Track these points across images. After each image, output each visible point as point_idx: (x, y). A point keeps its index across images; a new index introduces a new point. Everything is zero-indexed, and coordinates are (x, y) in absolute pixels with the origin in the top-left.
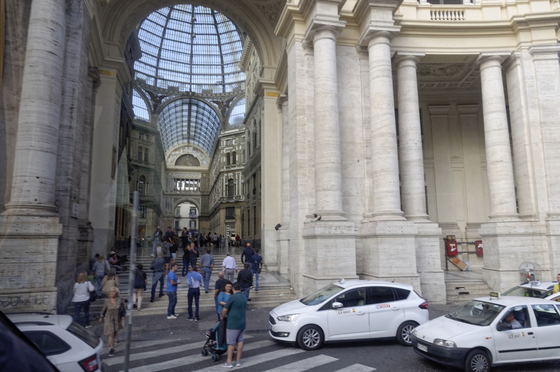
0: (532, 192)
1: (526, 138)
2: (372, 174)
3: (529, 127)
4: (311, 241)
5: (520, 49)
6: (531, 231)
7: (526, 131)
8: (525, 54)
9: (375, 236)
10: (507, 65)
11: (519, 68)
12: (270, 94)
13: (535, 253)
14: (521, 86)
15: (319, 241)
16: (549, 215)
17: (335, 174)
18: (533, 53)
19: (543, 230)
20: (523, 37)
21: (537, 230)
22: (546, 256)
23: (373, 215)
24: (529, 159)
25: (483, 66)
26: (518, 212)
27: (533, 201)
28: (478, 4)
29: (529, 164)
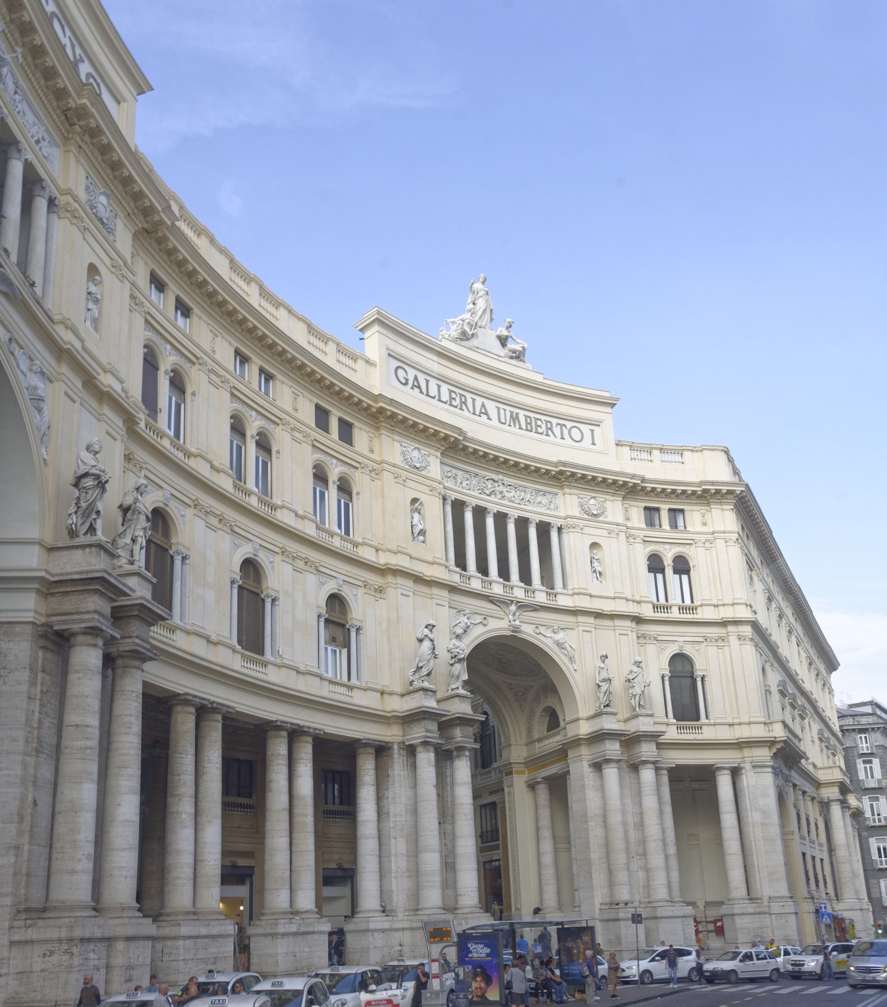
0: (758, 879)
1: (752, 835)
2: (647, 870)
3: (753, 827)
4: (611, 924)
5: (744, 762)
6: (758, 910)
7: (751, 829)
8: (748, 766)
9: (656, 918)
10: (735, 772)
11: (744, 776)
12: (518, 772)
13: (761, 928)
14: (746, 792)
15: (622, 923)
16: (770, 898)
17: (626, 872)
18: (754, 767)
19: (767, 910)
20: (747, 752)
21: (763, 910)
22: (769, 930)
23: (649, 902)
24: (754, 852)
25: (717, 773)
26: (749, 895)
27: (759, 886)
28: (712, 721)
29: (755, 857)
